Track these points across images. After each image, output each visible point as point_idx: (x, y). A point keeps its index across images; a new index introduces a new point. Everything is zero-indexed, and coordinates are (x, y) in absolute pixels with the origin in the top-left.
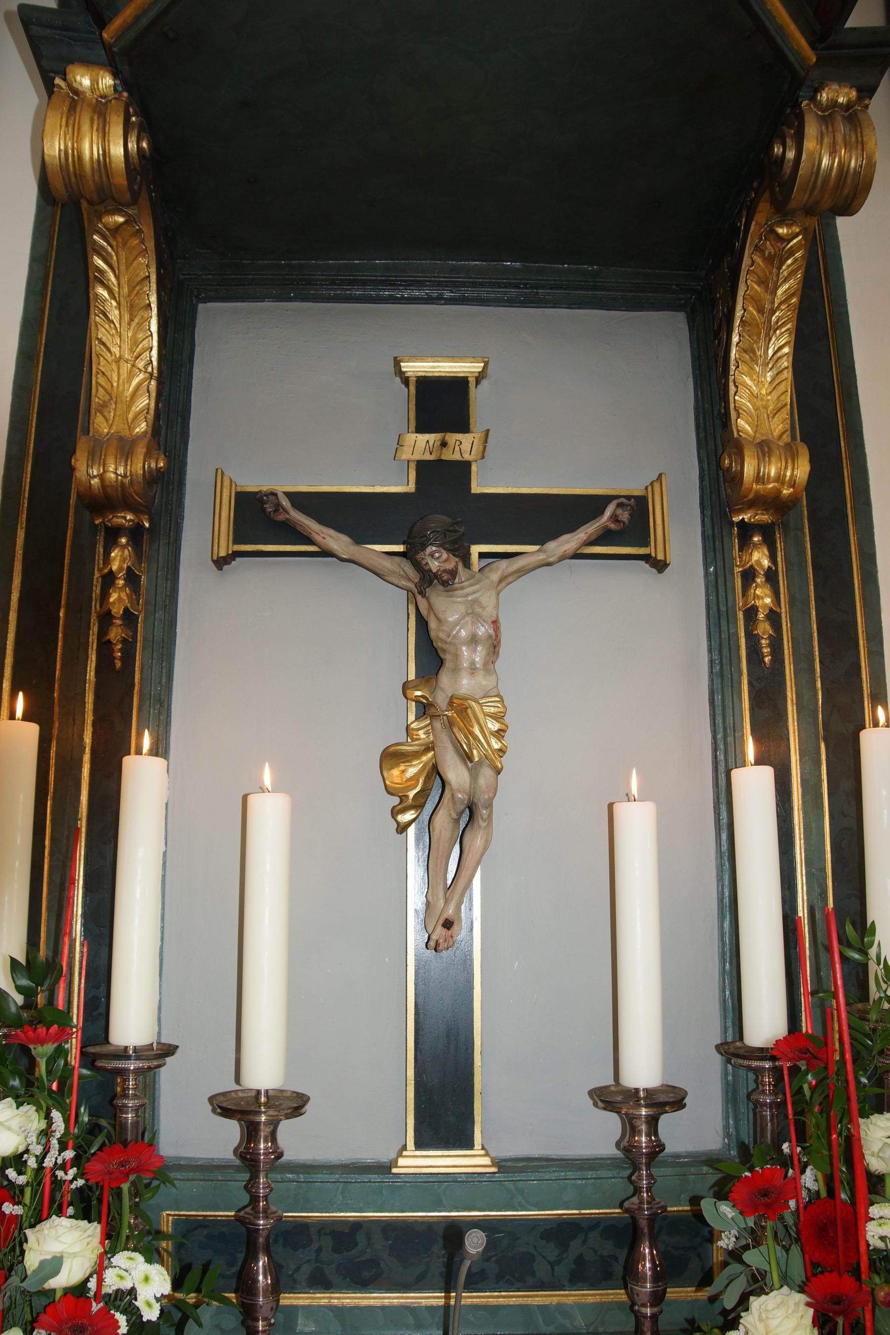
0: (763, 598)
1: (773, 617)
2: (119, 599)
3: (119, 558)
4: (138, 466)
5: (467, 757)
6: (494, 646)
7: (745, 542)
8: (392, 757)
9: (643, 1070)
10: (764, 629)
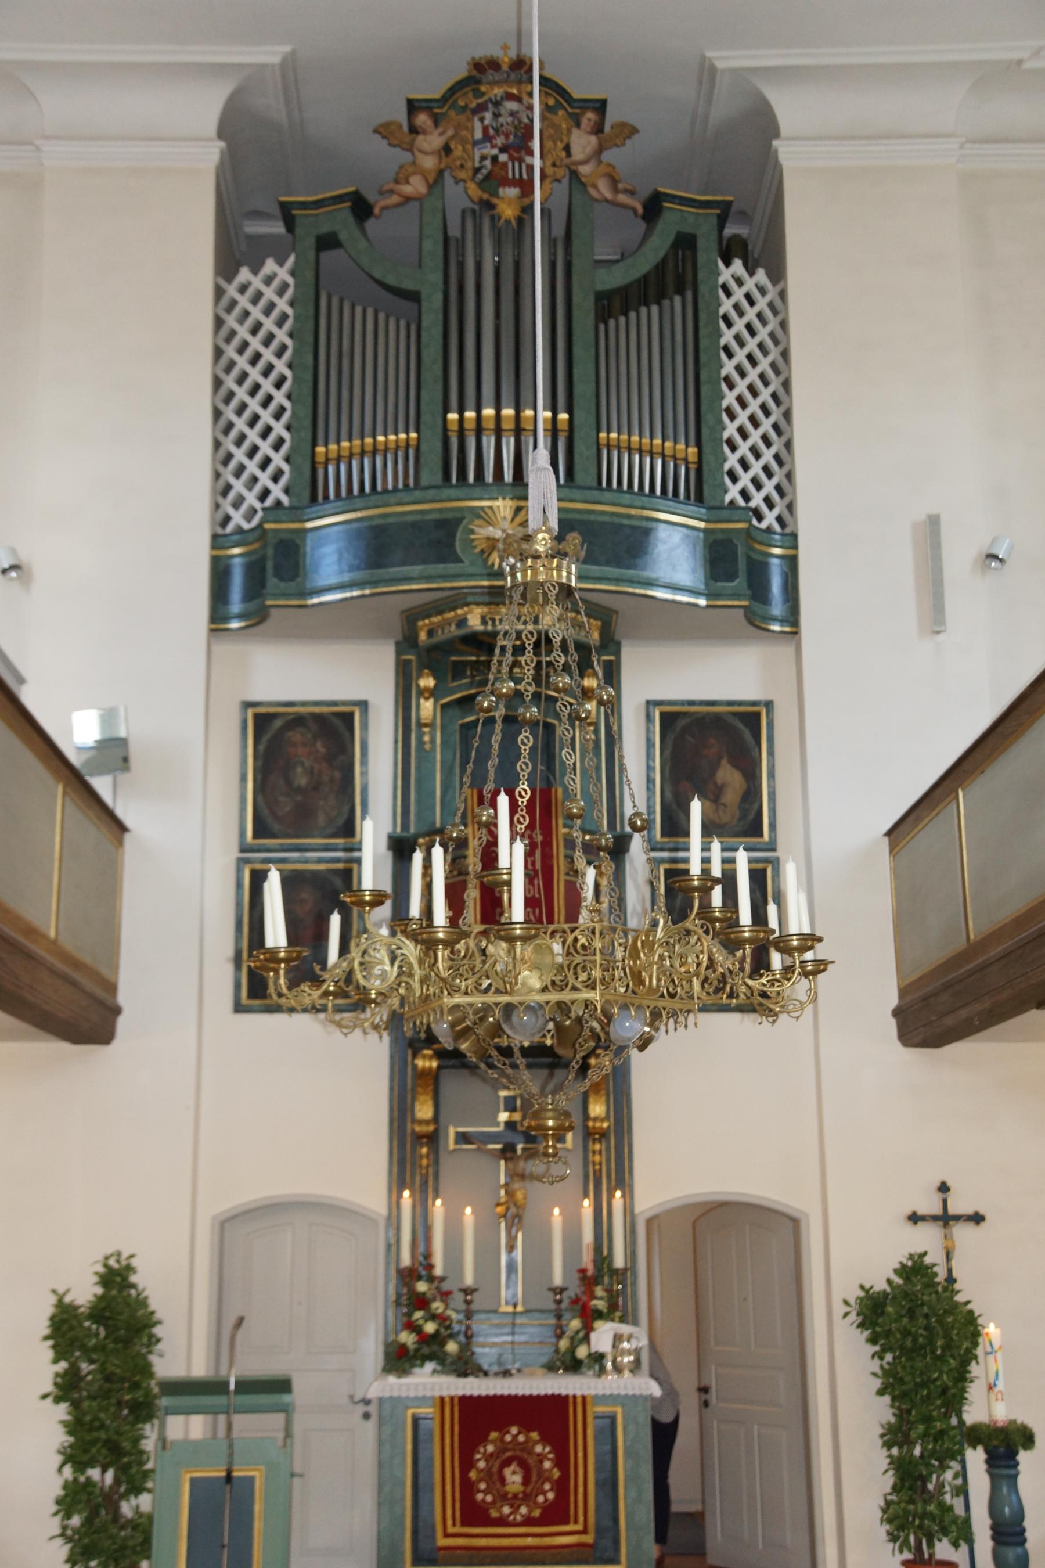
0: (597, 1158)
1: (600, 1164)
2: (425, 1162)
3: (424, 1150)
4: (431, 1128)
5: (515, 1205)
8: (498, 1205)
9: (558, 1280)
10: (597, 1167)
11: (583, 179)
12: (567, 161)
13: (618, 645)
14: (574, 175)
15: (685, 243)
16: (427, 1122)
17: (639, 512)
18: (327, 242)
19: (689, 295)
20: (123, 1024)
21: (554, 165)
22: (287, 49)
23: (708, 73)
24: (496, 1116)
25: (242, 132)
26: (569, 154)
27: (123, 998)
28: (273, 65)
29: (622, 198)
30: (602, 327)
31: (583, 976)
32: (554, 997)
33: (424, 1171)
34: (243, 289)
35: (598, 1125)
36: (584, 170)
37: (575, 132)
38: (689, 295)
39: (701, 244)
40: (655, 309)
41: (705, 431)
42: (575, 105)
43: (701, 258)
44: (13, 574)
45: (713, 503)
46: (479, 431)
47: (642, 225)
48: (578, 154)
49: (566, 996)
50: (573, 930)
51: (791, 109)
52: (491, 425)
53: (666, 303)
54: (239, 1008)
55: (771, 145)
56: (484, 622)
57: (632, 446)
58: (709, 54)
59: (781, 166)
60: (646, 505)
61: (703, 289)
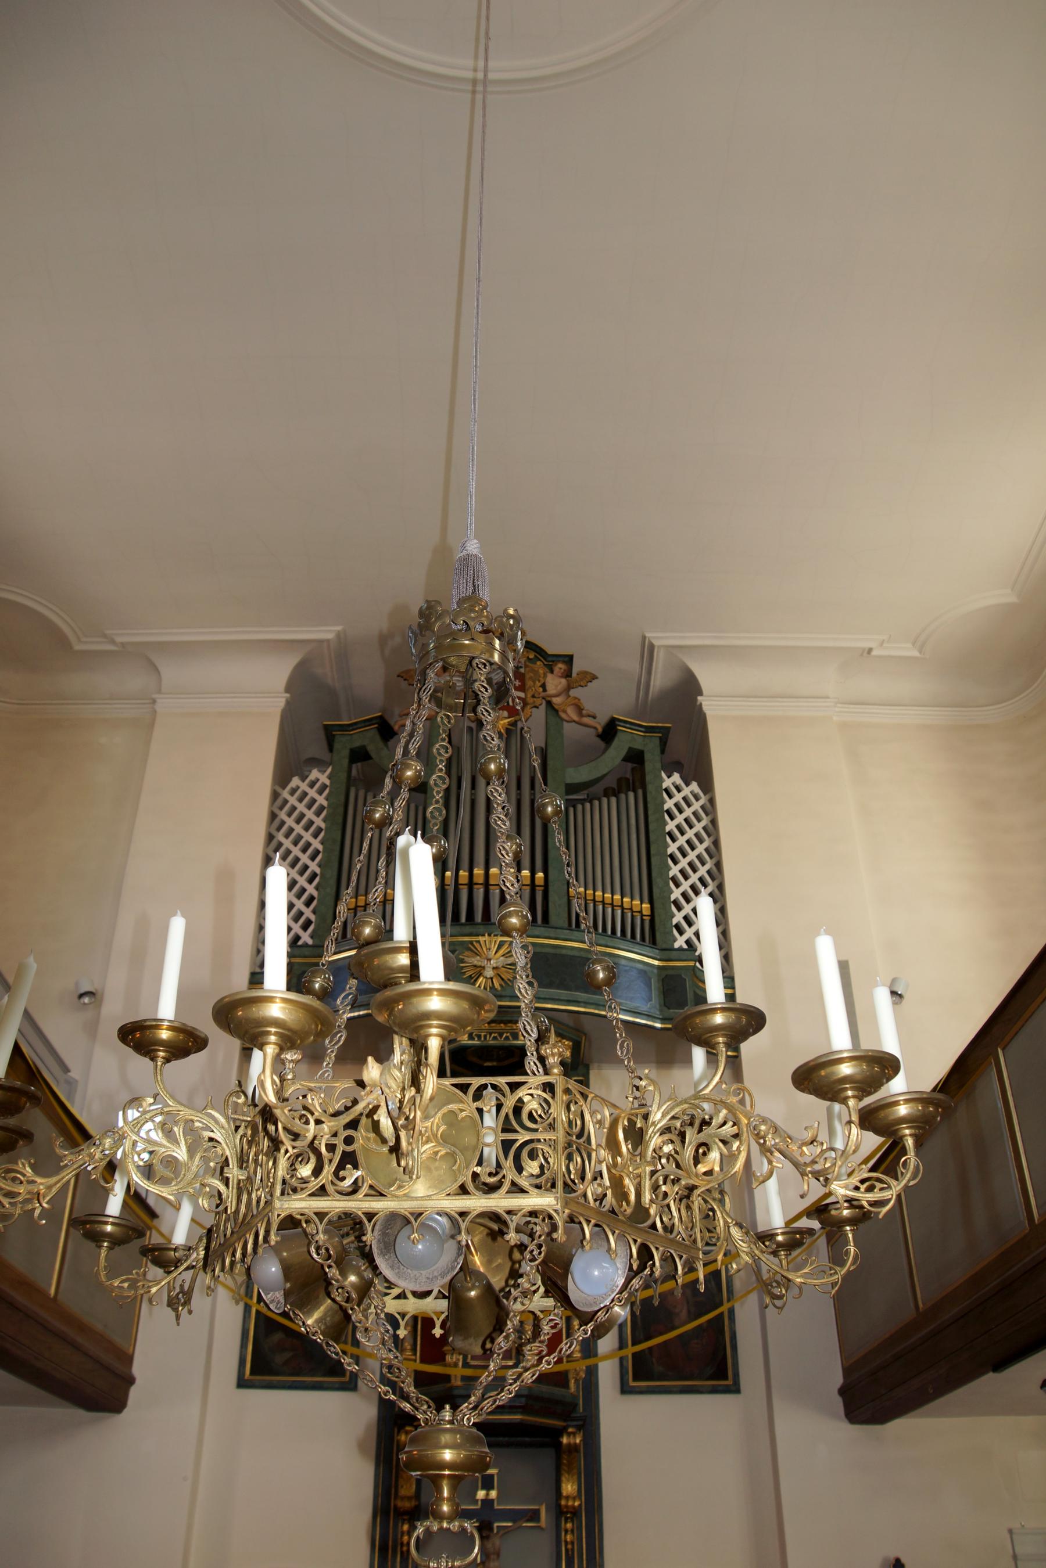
1: (572, 1543)
4: (413, 1503)
6: (498, 1555)
7: (566, 1522)
10: (569, 1546)
11: (556, 707)
12: (543, 694)
13: (587, 1068)
14: (549, 703)
15: (635, 757)
16: (409, 1498)
17: (603, 949)
18: (359, 755)
19: (640, 792)
20: (134, 1393)
21: (533, 696)
22: (339, 628)
23: (648, 651)
24: (475, 1494)
25: (304, 684)
26: (545, 690)
27: (136, 1370)
28: (328, 641)
29: (586, 720)
30: (571, 810)
31: (532, 1167)
32: (478, 1203)
33: (405, 1549)
34: (293, 792)
35: (570, 1503)
36: (555, 700)
37: (549, 675)
38: (640, 792)
39: (647, 756)
40: (613, 800)
41: (656, 891)
42: (550, 659)
43: (648, 766)
44: (86, 1000)
45: (664, 946)
46: (471, 884)
47: (602, 745)
48: (551, 689)
49: (499, 1202)
50: (514, 1087)
51: (707, 677)
52: (481, 880)
53: (623, 796)
54: (242, 1383)
55: (696, 700)
56: (471, 1037)
57: (597, 899)
58: (647, 635)
59: (705, 714)
60: (610, 944)
61: (650, 788)
